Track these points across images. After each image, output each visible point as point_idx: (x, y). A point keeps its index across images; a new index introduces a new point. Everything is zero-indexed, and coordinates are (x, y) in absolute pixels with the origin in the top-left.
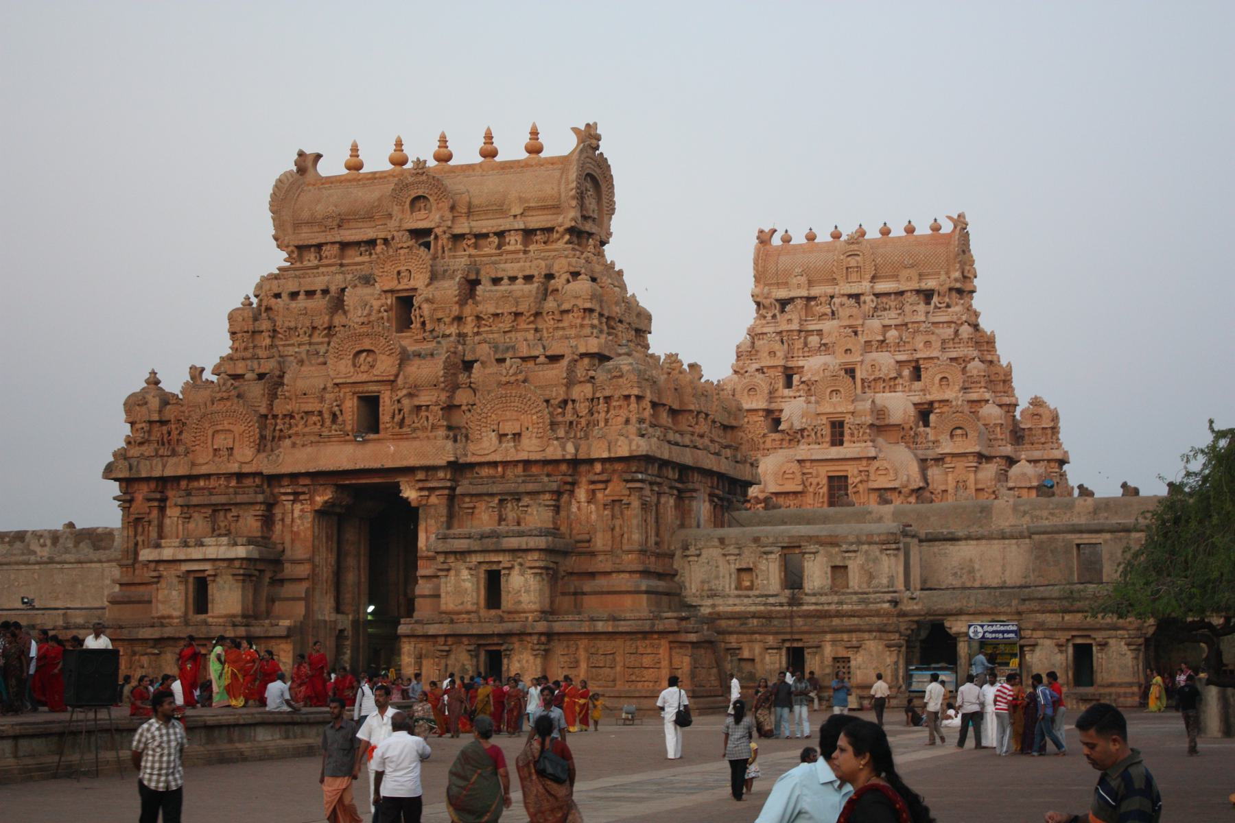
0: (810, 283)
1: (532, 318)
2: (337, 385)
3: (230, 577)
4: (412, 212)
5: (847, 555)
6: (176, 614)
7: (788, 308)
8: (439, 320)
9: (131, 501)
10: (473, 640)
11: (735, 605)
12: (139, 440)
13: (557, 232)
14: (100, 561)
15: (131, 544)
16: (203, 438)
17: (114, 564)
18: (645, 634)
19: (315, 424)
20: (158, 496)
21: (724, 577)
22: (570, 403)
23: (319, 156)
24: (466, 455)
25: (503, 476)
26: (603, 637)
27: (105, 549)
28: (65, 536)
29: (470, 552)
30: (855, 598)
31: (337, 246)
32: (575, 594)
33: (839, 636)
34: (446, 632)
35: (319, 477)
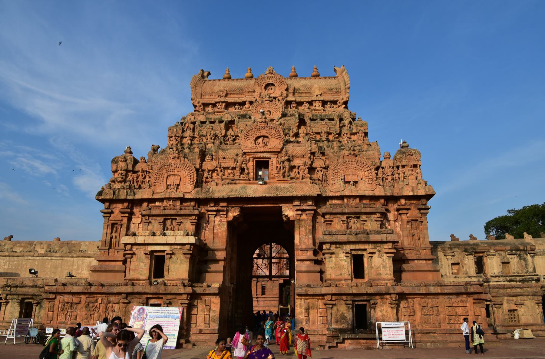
2: (244, 153)
3: (182, 256)
4: (265, 91)
5: (510, 256)
6: (141, 277)
12: (119, 179)
14: (73, 257)
16: (162, 178)
18: (458, 294)
20: (129, 210)
21: (445, 267)
22: (380, 168)
23: (209, 74)
24: (326, 192)
30: (518, 278)
33: (511, 298)
34: (333, 292)
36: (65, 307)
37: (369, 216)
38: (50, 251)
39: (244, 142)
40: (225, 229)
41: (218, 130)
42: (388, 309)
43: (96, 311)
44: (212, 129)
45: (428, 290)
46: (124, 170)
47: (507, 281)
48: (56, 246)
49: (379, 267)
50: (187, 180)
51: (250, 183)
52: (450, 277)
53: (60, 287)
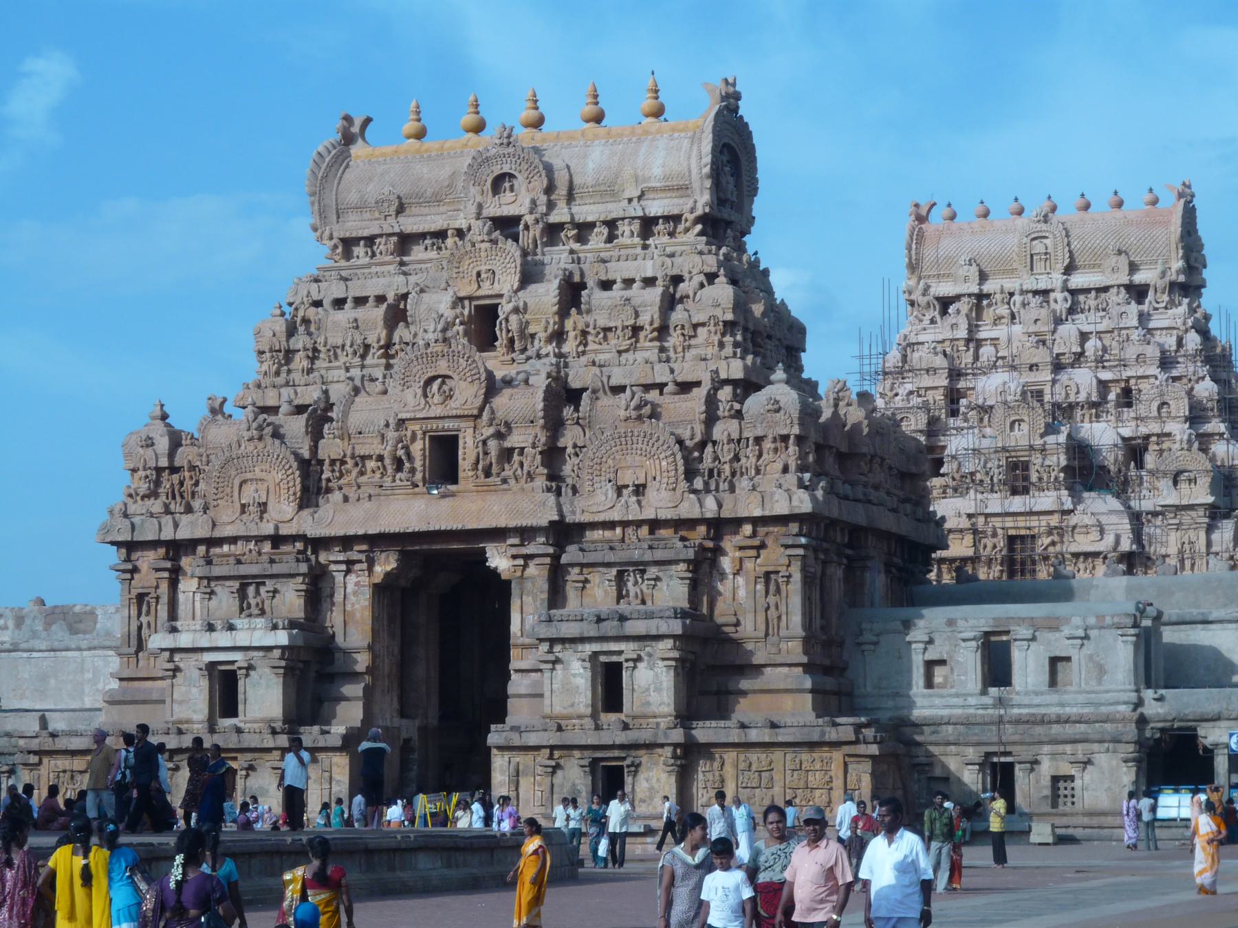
0: (983, 277)
1: (655, 334)
3: (268, 670)
6: (196, 717)
7: (951, 310)
8: (533, 336)
10: (587, 753)
13: (686, 220)
14: (79, 649)
15: (134, 628)
17: (111, 653)
18: (812, 745)
19: (373, 472)
20: (168, 565)
22: (709, 448)
23: (368, 121)
24: (574, 513)
25: (623, 540)
27: (85, 632)
28: (32, 615)
29: (582, 640)
31: (395, 239)
32: (718, 693)
33: (1060, 748)
34: (552, 742)
35: (378, 541)
36: (61, 780)
37: (666, 567)
39: (399, 393)
40: (367, 603)
49: (648, 689)
50: (282, 492)
53: (46, 740)
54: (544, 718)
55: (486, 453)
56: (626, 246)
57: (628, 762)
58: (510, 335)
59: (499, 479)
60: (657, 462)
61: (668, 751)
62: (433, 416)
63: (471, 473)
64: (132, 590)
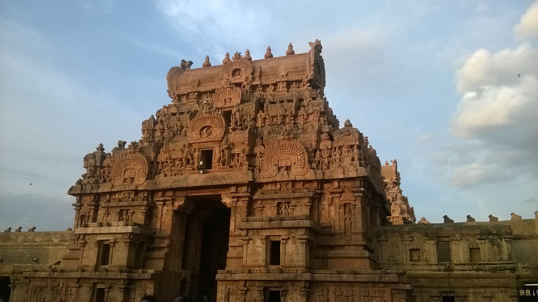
3: (123, 244)
9: (82, 205)
11: (410, 270)
22: (318, 152)
23: (191, 63)
24: (259, 178)
25: (280, 190)
26: (346, 284)
29: (262, 229)
30: (487, 267)
32: (323, 258)
33: (478, 290)
34: (246, 278)
36: (37, 290)
38: (62, 241)
40: (170, 218)
41: (184, 121)
42: (299, 296)
43: (58, 294)
44: (179, 120)
45: (340, 277)
46: (92, 166)
47: (473, 269)
48: (67, 236)
49: (292, 254)
51: (194, 173)
52: (406, 265)
54: (242, 266)
55: (224, 156)
56: (281, 91)
57: (282, 289)
58: (236, 120)
59: (228, 166)
60: (296, 156)
61: (302, 284)
62: (203, 141)
63: (217, 164)
64: (80, 214)
